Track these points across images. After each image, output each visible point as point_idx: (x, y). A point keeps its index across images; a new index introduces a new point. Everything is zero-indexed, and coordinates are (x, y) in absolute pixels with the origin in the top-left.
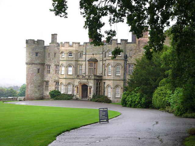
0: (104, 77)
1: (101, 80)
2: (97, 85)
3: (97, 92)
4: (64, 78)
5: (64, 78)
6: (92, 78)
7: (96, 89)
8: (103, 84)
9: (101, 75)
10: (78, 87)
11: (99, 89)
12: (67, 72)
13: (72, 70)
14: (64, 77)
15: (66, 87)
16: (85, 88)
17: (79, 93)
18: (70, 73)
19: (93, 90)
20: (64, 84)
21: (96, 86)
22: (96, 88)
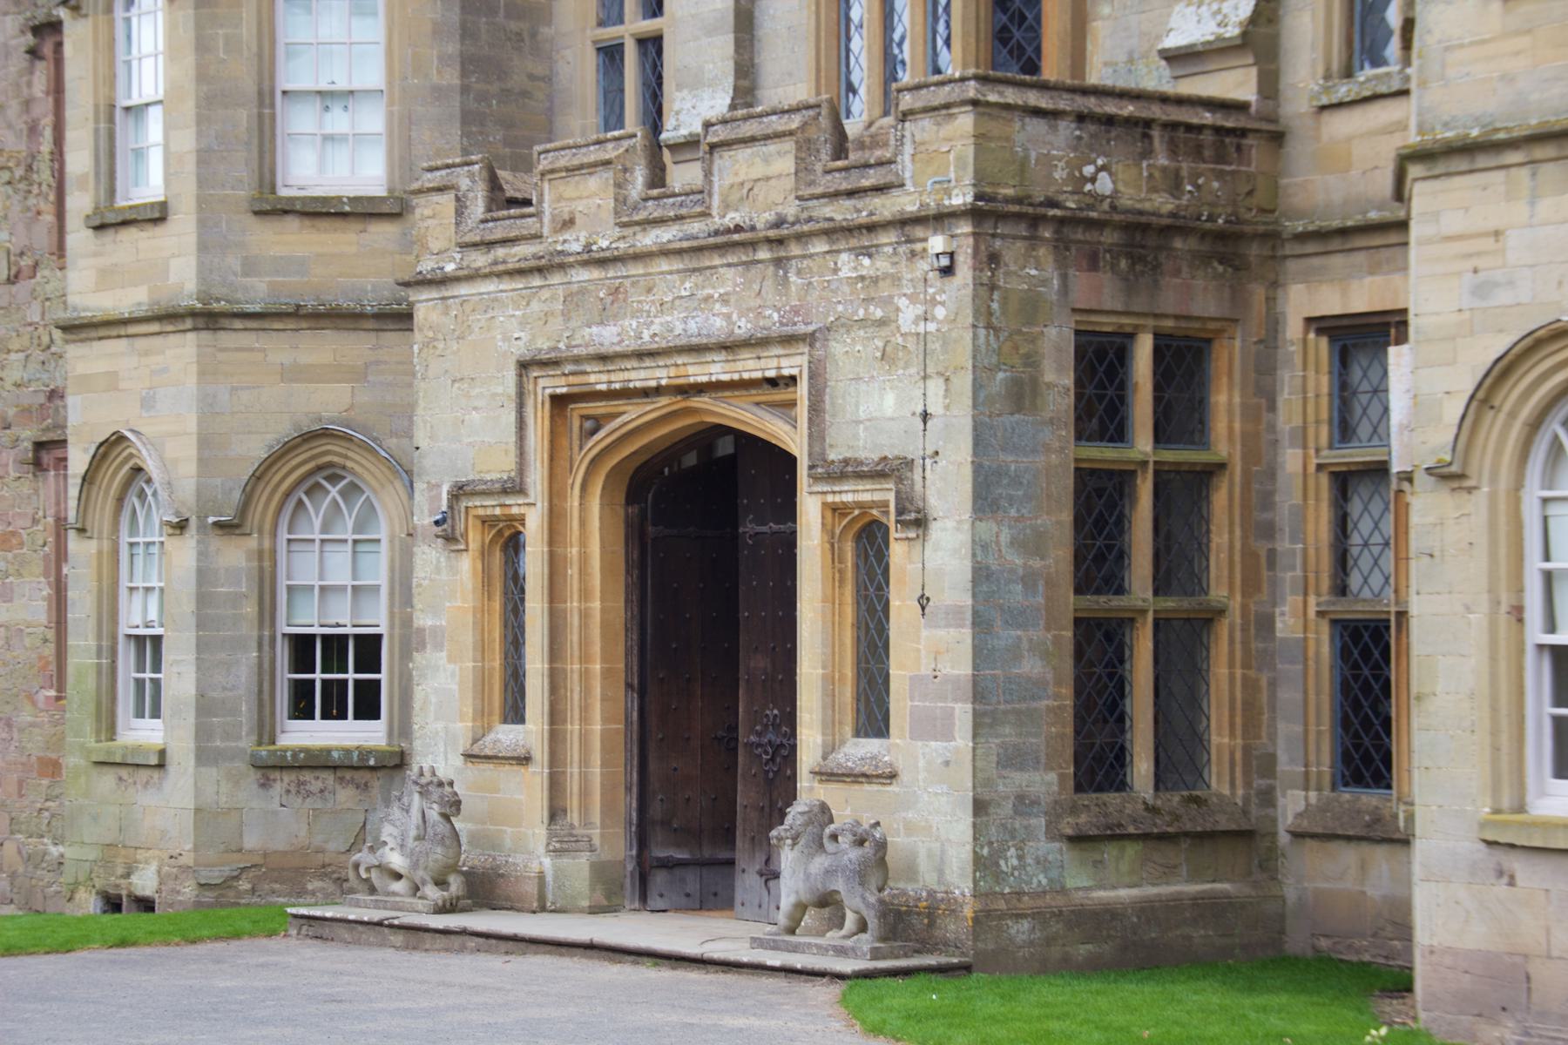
0: (1341, 157)
1: (1246, 245)
2: (1100, 409)
3: (1098, 649)
4: (168, 317)
5: (168, 317)
6: (905, 202)
7: (1060, 557)
8: (1305, 379)
9: (1236, 83)
10: (513, 544)
11: (1179, 562)
12: (243, 117)
13: (372, 75)
14: (173, 264)
15: (235, 555)
16: (704, 530)
17: (532, 733)
18: (341, 155)
19: (954, 590)
20: (187, 488)
21: (1053, 450)
22: (1058, 521)
